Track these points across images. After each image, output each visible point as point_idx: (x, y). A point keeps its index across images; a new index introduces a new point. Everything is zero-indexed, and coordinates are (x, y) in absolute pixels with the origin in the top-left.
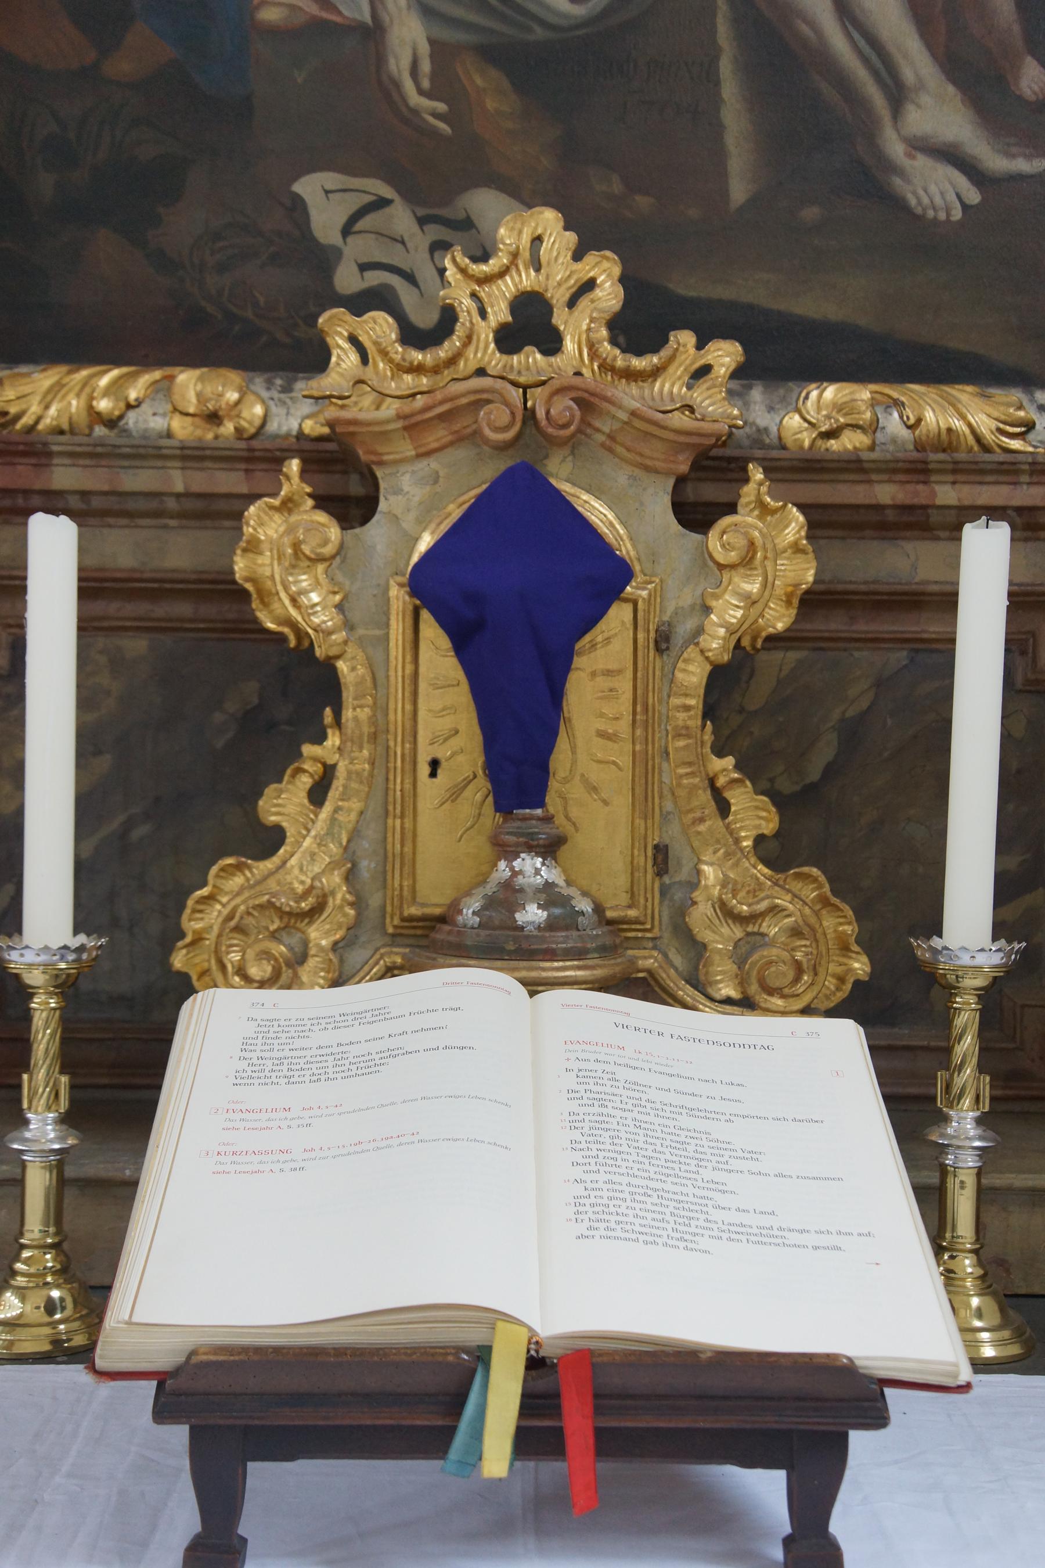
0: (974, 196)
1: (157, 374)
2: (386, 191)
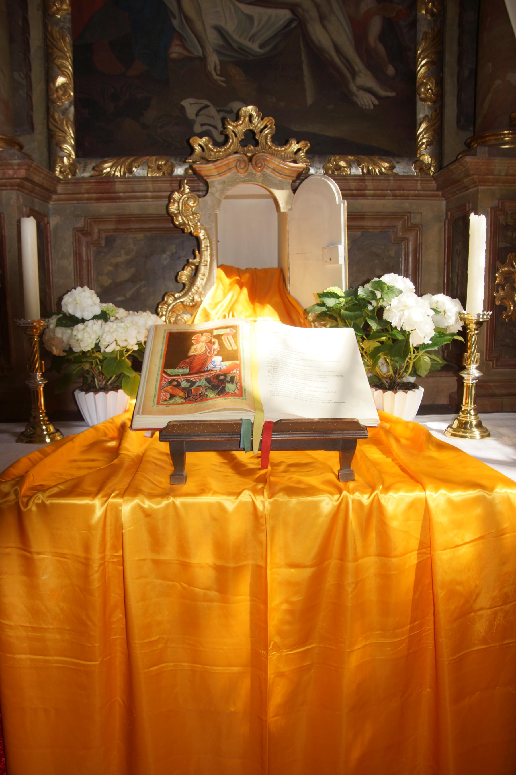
0: (376, 102)
2: (208, 103)
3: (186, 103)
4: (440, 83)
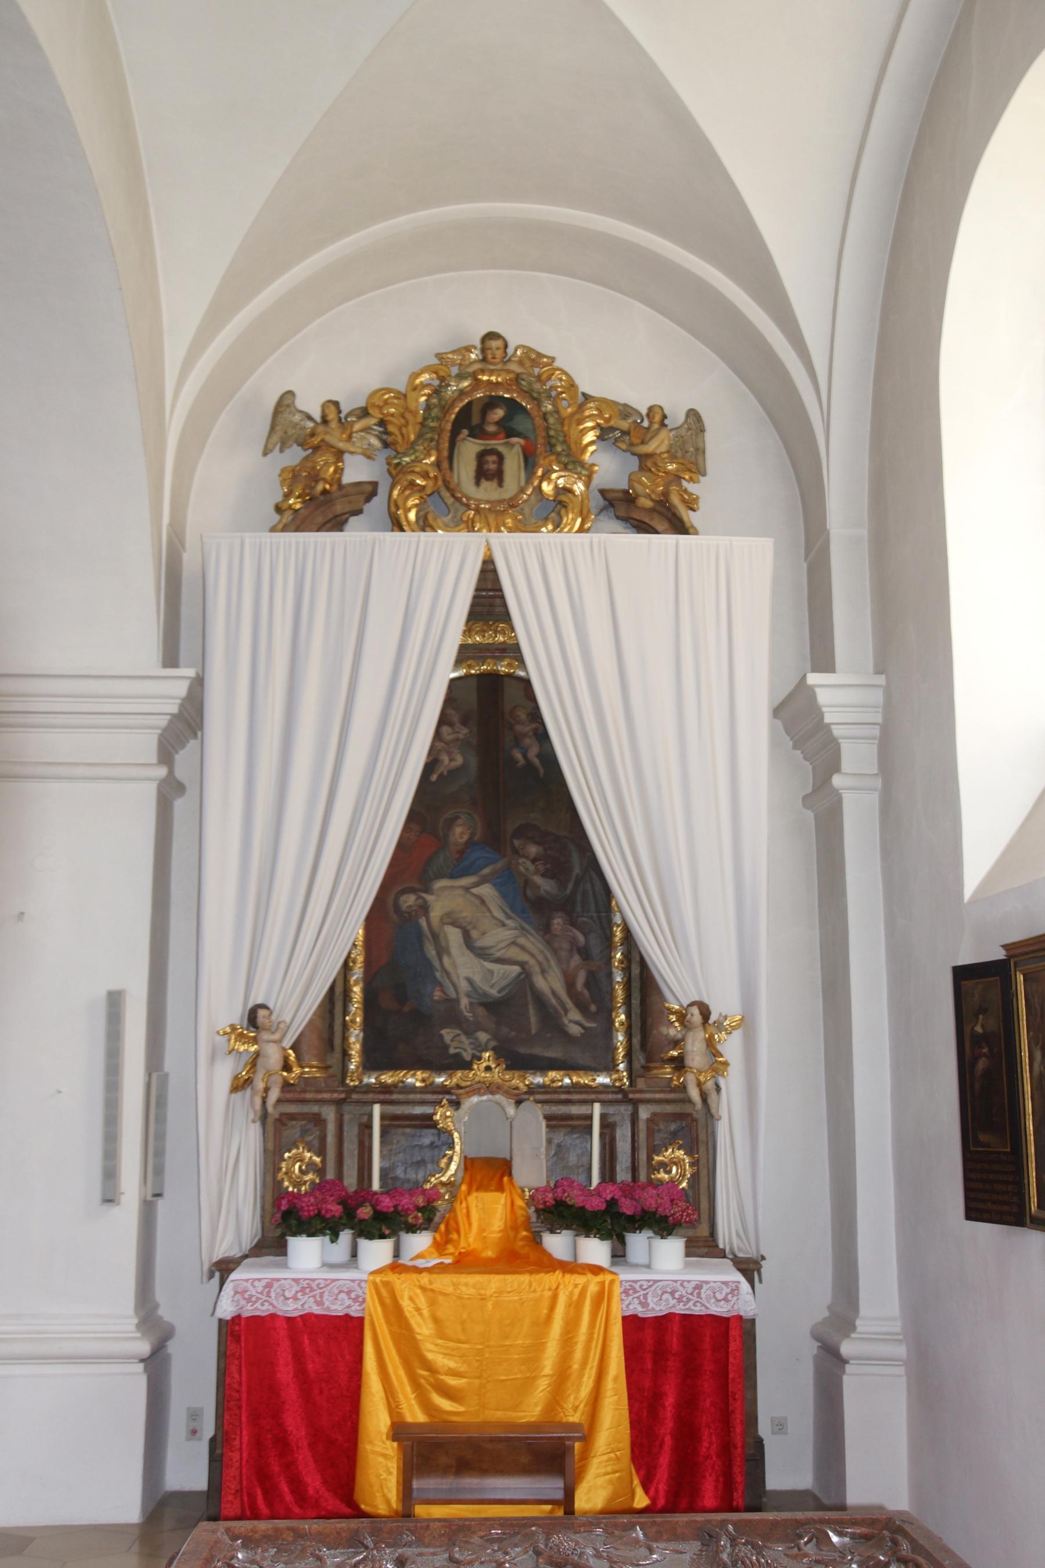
0: (583, 1031)
1: (412, 1072)
2: (458, 1032)
3: (444, 1032)
4: (629, 1016)
